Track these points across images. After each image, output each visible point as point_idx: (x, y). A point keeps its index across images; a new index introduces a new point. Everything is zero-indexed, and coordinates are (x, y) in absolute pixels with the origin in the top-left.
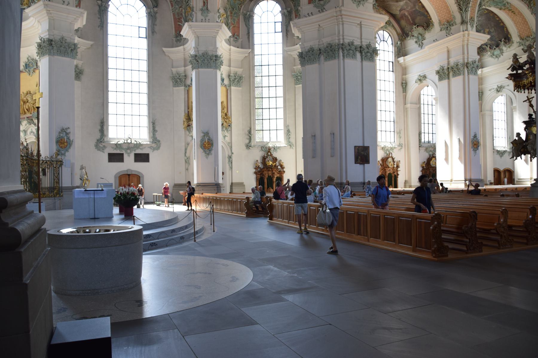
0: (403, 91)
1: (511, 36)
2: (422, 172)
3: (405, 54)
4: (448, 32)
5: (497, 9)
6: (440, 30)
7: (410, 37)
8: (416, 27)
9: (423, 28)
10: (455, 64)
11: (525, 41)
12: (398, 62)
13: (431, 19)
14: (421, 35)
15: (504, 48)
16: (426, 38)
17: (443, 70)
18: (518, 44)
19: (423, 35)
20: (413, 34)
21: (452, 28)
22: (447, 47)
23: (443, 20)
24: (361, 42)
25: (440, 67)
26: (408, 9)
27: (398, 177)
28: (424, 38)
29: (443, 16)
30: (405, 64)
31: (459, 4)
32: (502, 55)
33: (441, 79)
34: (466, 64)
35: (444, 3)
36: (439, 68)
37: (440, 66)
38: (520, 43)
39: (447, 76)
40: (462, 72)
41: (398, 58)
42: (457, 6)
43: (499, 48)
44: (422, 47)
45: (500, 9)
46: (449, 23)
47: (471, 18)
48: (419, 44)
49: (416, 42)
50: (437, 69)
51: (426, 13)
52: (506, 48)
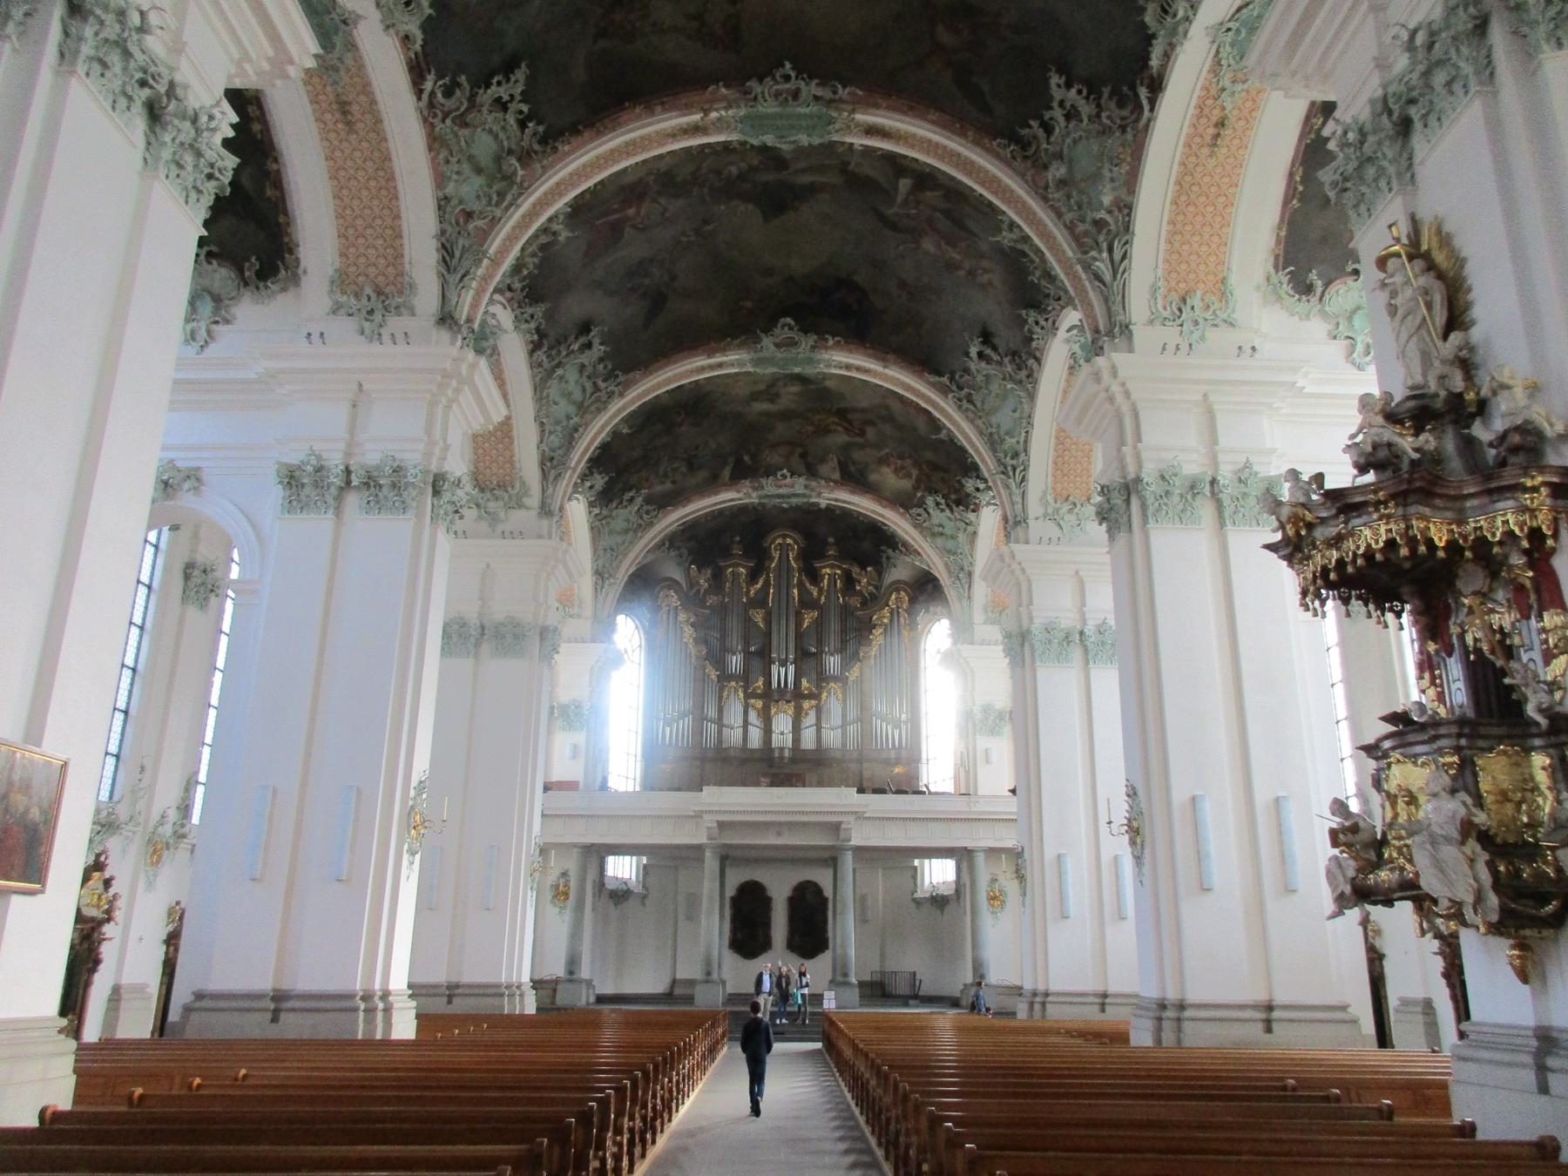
14: (217, 299)
19: (227, 302)
28: (229, 317)
29: (362, 260)
31: (448, 246)
39: (330, 500)
42: (438, 250)
50: (294, 458)
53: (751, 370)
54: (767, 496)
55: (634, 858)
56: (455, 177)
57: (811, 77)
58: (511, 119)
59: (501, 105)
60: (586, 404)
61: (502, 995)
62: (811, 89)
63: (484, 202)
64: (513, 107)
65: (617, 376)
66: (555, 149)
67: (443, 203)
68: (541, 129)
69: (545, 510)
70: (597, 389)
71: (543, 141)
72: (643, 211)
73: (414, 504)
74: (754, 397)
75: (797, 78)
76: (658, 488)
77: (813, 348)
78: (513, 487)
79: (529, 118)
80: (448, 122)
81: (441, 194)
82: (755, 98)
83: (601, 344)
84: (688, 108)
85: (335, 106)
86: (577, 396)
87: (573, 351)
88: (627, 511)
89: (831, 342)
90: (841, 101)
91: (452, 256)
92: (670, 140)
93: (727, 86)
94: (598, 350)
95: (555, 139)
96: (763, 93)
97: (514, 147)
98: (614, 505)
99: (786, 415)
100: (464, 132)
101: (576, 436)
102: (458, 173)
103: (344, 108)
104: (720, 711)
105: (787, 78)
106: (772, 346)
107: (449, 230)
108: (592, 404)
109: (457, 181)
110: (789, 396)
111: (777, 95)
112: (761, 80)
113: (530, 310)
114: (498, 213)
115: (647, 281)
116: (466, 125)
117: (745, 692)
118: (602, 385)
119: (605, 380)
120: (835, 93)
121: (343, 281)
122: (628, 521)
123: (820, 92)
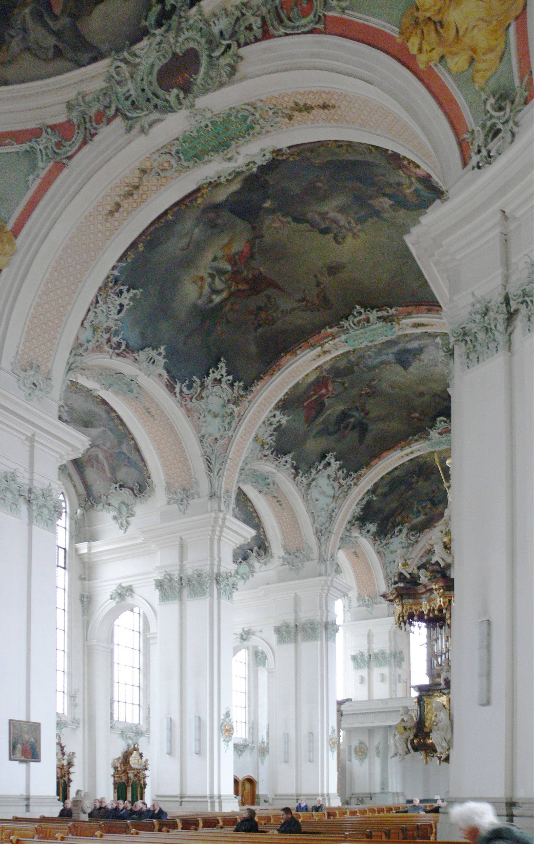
0: (83, 612)
1: (269, 544)
3: (91, 538)
4: (182, 510)
5: (255, 490)
6: (166, 503)
7: (103, 505)
8: (118, 488)
9: (131, 492)
10: (196, 572)
11: (292, 556)
12: (76, 550)
13: (149, 477)
14: (127, 505)
15: (257, 565)
17: (171, 580)
20: (109, 502)
21: (191, 502)
22: (181, 538)
25: (165, 575)
26: (105, 448)
28: (133, 513)
29: (175, 475)
30: (90, 558)
31: (208, 458)
32: (253, 576)
35: (179, 450)
36: (163, 575)
40: (208, 590)
41: (75, 544)
42: (204, 462)
43: (248, 563)
44: (126, 529)
45: (260, 492)
46: (186, 492)
47: (227, 491)
49: (115, 518)
51: (141, 464)
52: (260, 564)
56: (204, 424)
57: (373, 308)
59: (218, 381)
60: (336, 495)
62: (373, 315)
63: (222, 429)
65: (351, 475)
67: (202, 439)
68: (241, 384)
69: (322, 559)
71: (245, 388)
72: (330, 388)
73: (208, 590)
75: (365, 311)
76: (416, 521)
78: (304, 550)
79: (234, 381)
80: (194, 400)
81: (200, 435)
82: (348, 329)
83: (335, 461)
84: (313, 346)
86: (331, 492)
87: (320, 470)
88: (400, 537)
90: (393, 315)
92: (313, 362)
93: (330, 328)
95: (251, 386)
96: (350, 325)
97: (230, 398)
98: (389, 536)
100: (202, 403)
101: (334, 514)
102: (205, 422)
105: (360, 313)
107: (208, 450)
108: (340, 494)
109: (206, 426)
111: (359, 322)
112: (347, 319)
113: (283, 460)
114: (230, 433)
115: (352, 420)
116: (202, 398)
119: (344, 479)
120: (388, 312)
121: (169, 487)
123: (380, 314)
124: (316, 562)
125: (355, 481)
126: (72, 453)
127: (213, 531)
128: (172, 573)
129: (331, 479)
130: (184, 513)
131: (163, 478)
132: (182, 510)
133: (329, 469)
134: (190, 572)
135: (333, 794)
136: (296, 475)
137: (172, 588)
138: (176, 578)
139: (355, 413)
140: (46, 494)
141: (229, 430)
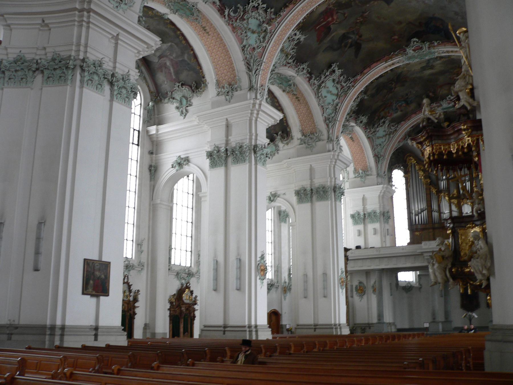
1: (290, 129)
2: (170, 311)
3: (159, 122)
4: (228, 99)
5: (280, 90)
6: (216, 95)
7: (169, 99)
8: (180, 86)
9: (190, 89)
12: (148, 132)
13: (204, 77)
14: (187, 99)
15: (281, 145)
16: (193, 104)
17: (218, 151)
18: (299, 141)
19: (189, 99)
20: (173, 96)
21: (235, 93)
22: (227, 120)
23: (231, 75)
24: (115, 67)
25: (214, 147)
26: (172, 58)
27: (134, 318)
28: (191, 104)
29: (223, 75)
30: (157, 138)
31: (248, 62)
32: (278, 153)
33: (214, 164)
34: (253, 147)
36: (213, 148)
37: (214, 146)
38: (301, 140)
40: (248, 158)
41: (147, 127)
43: (274, 143)
44: (185, 115)
45: (284, 91)
46: (231, 86)
47: (262, 86)
48: (182, 111)
49: (177, 108)
51: (198, 68)
52: (283, 145)
53: (408, 62)
54: (445, 109)
55: (414, 272)
56: (245, 38)
58: (261, 11)
61: (333, 328)
63: (258, 42)
64: (260, 7)
65: (350, 80)
66: (280, 15)
67: (243, 49)
68: (273, 10)
70: (343, 87)
72: (335, 17)
74: (424, 69)
77: (429, 48)
79: (267, 8)
80: (238, 21)
81: (242, 45)
83: (339, 69)
85: (201, 29)
86: (335, 91)
87: (327, 76)
89: (436, 44)
91: (250, 65)
94: (338, 72)
95: (280, 11)
99: (442, 73)
102: (246, 36)
103: (204, 29)
104: (439, 206)
106: (411, 51)
107: (248, 56)
110: (438, 66)
115: (350, 41)
116: (244, 19)
117: (449, 197)
118: (344, 85)
119: (345, 82)
121: (218, 84)
122: (385, 131)
124: (325, 142)
125: (352, 84)
126: (147, 50)
127: (252, 114)
128: (219, 146)
129: (336, 82)
130: (230, 102)
131: (214, 77)
132: (228, 99)
133: (334, 75)
134: (233, 144)
135: (344, 324)
136: (310, 79)
137: (219, 157)
138: (223, 149)
139: (352, 36)
140: (125, 78)
141: (263, 42)
